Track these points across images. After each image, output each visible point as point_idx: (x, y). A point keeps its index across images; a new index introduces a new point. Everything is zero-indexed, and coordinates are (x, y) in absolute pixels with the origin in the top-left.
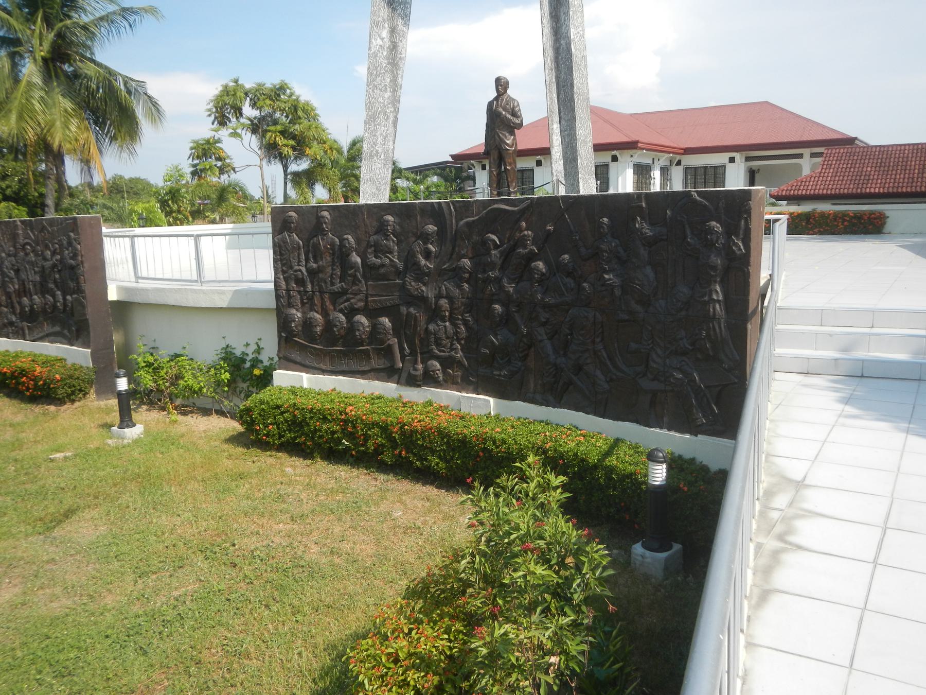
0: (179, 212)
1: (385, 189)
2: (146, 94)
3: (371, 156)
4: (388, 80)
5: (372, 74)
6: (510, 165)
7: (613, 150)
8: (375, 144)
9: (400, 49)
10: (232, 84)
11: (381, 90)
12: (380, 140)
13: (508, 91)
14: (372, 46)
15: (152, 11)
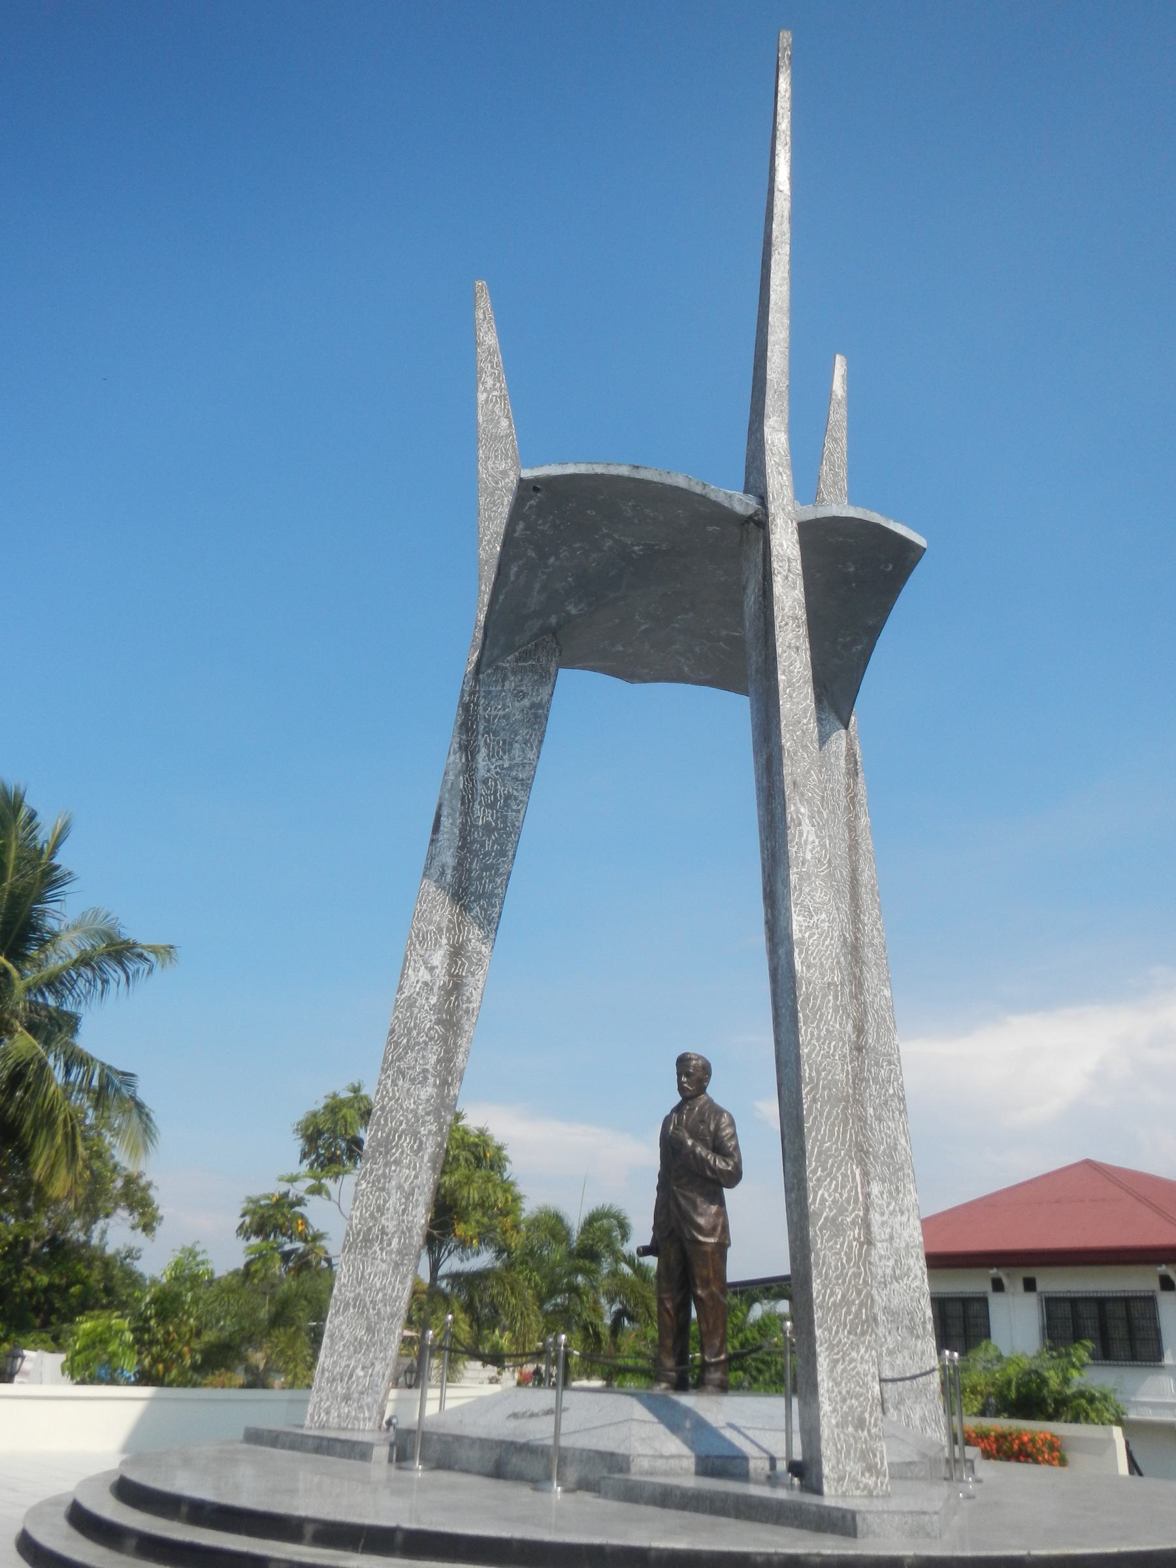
0: (167, 1344)
1: (390, 1331)
2: (133, 1098)
3: (367, 1241)
4: (433, 1059)
5: (397, 1044)
6: (706, 1283)
7: (1159, 1262)
8: (381, 1209)
9: (467, 991)
10: (346, 1095)
11: (413, 1081)
12: (394, 1200)
13: (708, 1090)
14: (407, 983)
15: (167, 951)
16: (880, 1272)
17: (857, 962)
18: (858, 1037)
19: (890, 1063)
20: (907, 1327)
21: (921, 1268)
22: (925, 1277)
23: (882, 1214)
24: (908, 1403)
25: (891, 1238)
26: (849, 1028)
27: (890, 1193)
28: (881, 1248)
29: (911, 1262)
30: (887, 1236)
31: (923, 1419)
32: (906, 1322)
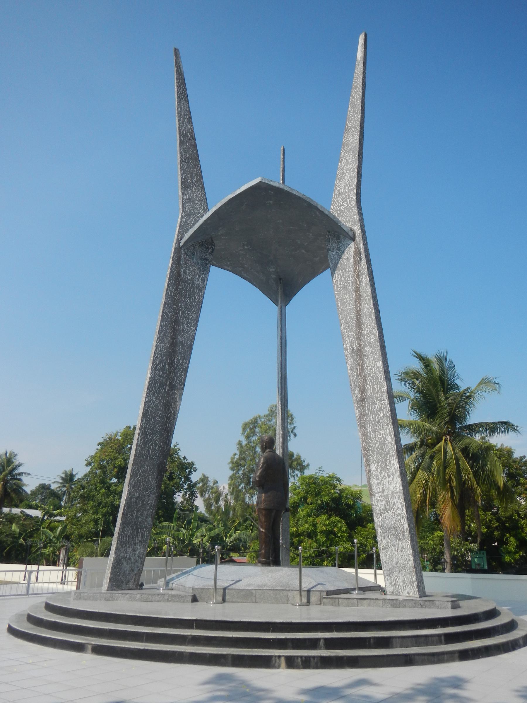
16: (378, 508)
17: (360, 357)
18: (362, 394)
19: (381, 400)
20: (394, 535)
21: (401, 503)
22: (404, 508)
23: (378, 479)
24: (396, 573)
25: (383, 490)
26: (357, 392)
27: (382, 467)
28: (377, 496)
29: (395, 501)
30: (381, 490)
31: (404, 582)
32: (393, 532)
